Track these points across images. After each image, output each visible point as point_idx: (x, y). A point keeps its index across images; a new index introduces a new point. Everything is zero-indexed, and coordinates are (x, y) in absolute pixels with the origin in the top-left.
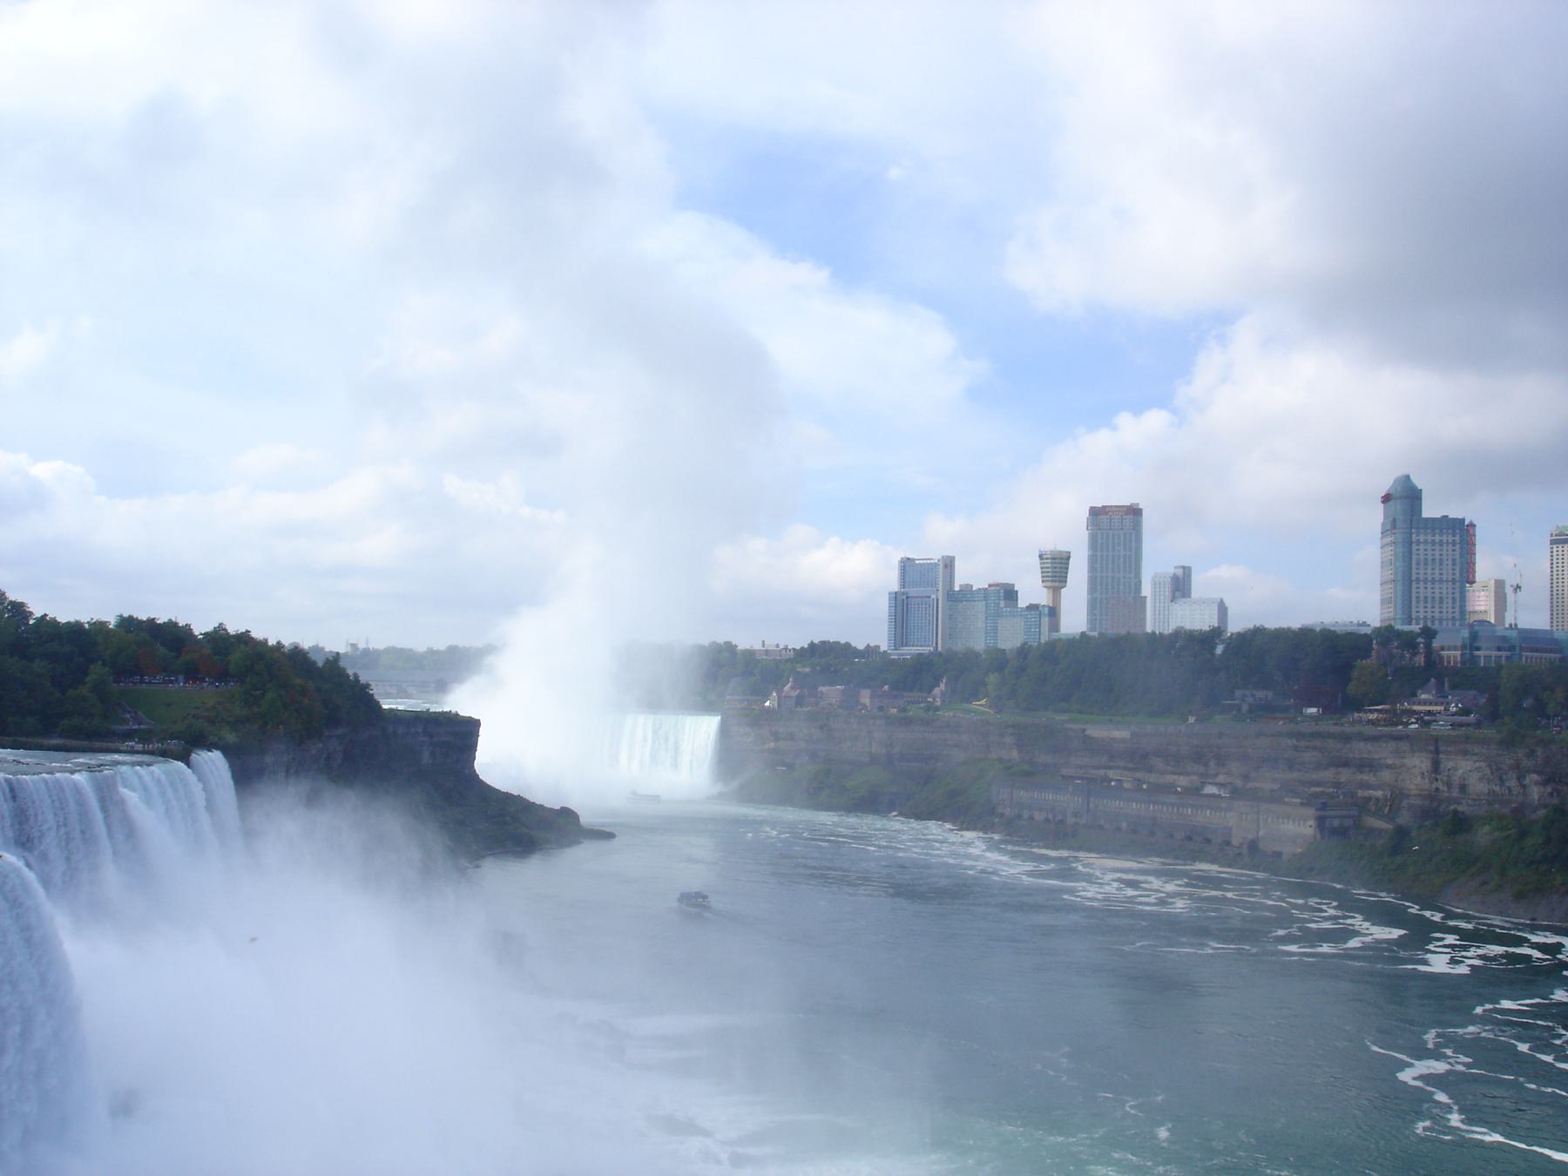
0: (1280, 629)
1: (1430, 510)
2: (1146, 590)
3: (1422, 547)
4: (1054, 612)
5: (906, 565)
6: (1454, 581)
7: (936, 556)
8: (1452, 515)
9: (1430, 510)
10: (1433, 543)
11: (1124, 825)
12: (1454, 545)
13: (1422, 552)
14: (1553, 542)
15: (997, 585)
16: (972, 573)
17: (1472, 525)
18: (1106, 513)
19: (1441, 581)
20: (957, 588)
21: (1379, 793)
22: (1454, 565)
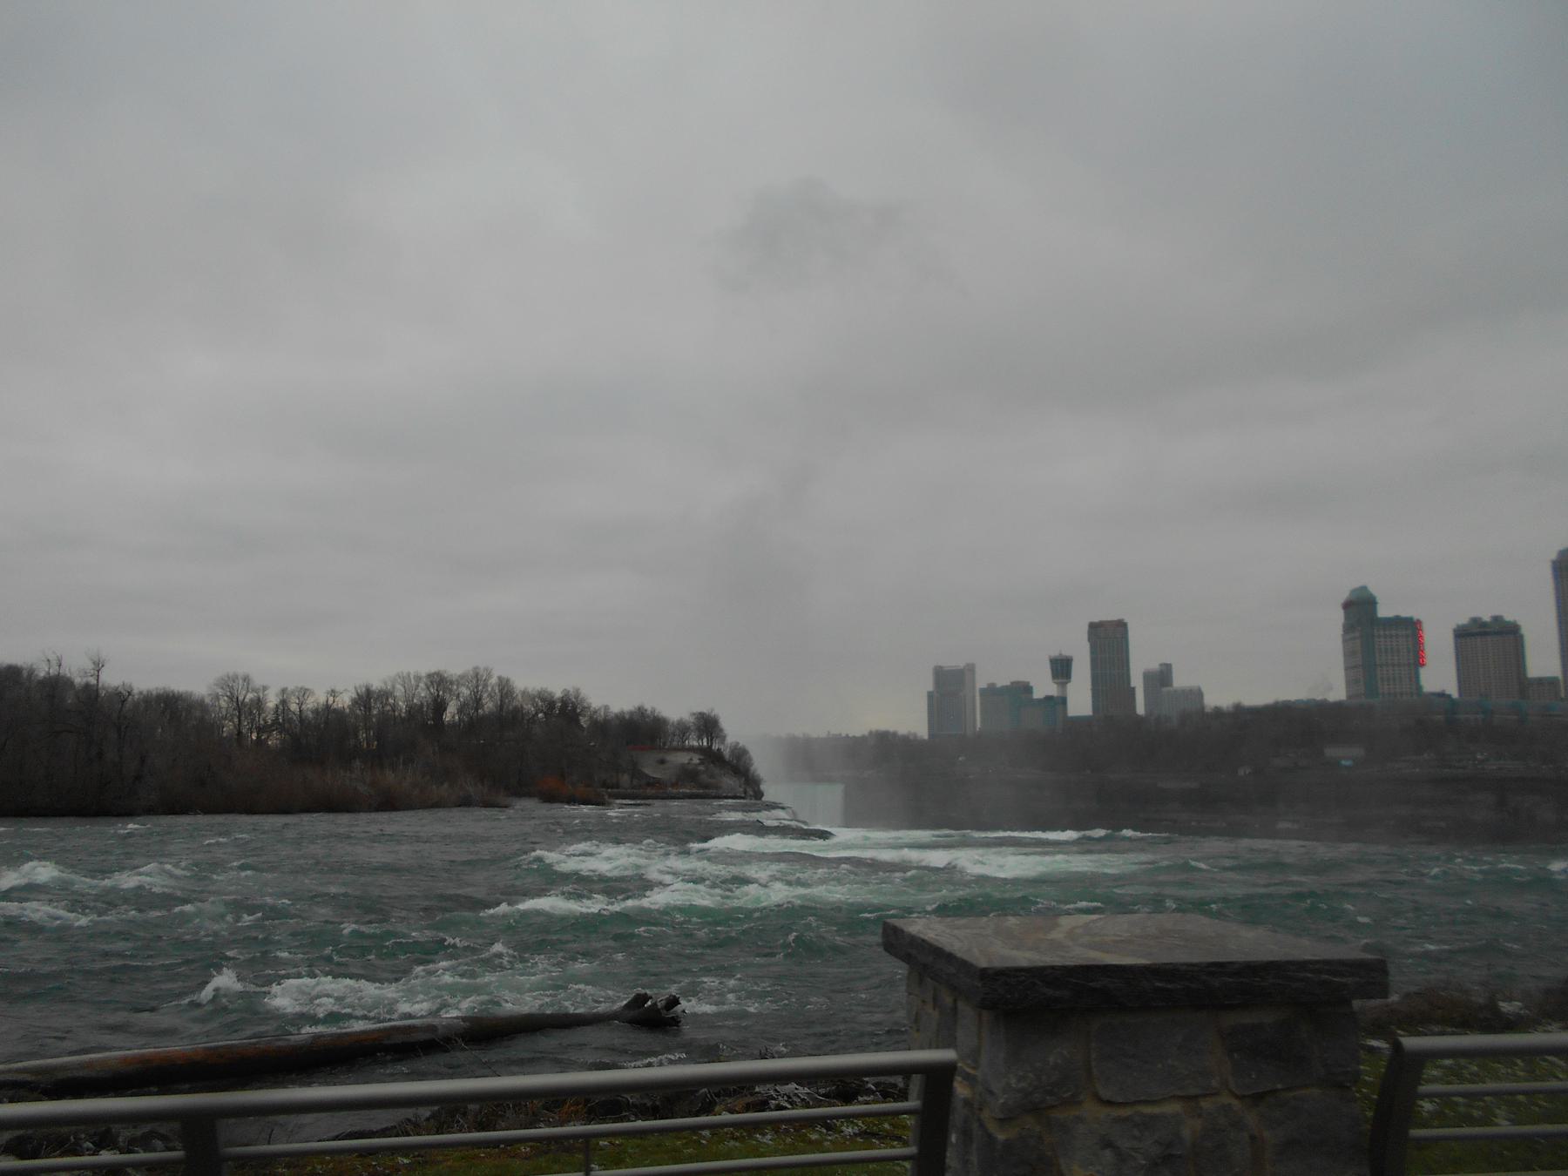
0: (1277, 703)
1: (1384, 611)
2: (1137, 682)
3: (1382, 640)
4: (1063, 701)
6: (1409, 664)
7: (961, 664)
8: (1404, 614)
9: (1384, 611)
15: (1018, 683)
16: (994, 673)
17: (1419, 622)
20: (981, 683)
21: (1443, 824)
22: (1409, 652)
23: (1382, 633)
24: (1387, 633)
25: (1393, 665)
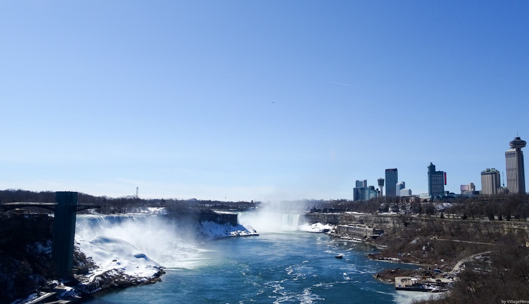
1: (437, 170)
3: (434, 178)
5: (357, 182)
8: (441, 171)
9: (437, 170)
10: (436, 177)
11: (352, 234)
12: (441, 176)
13: (434, 179)
14: (482, 174)
15: (370, 186)
18: (389, 171)
19: (438, 185)
23: (434, 176)
24: (435, 176)
25: (436, 185)
